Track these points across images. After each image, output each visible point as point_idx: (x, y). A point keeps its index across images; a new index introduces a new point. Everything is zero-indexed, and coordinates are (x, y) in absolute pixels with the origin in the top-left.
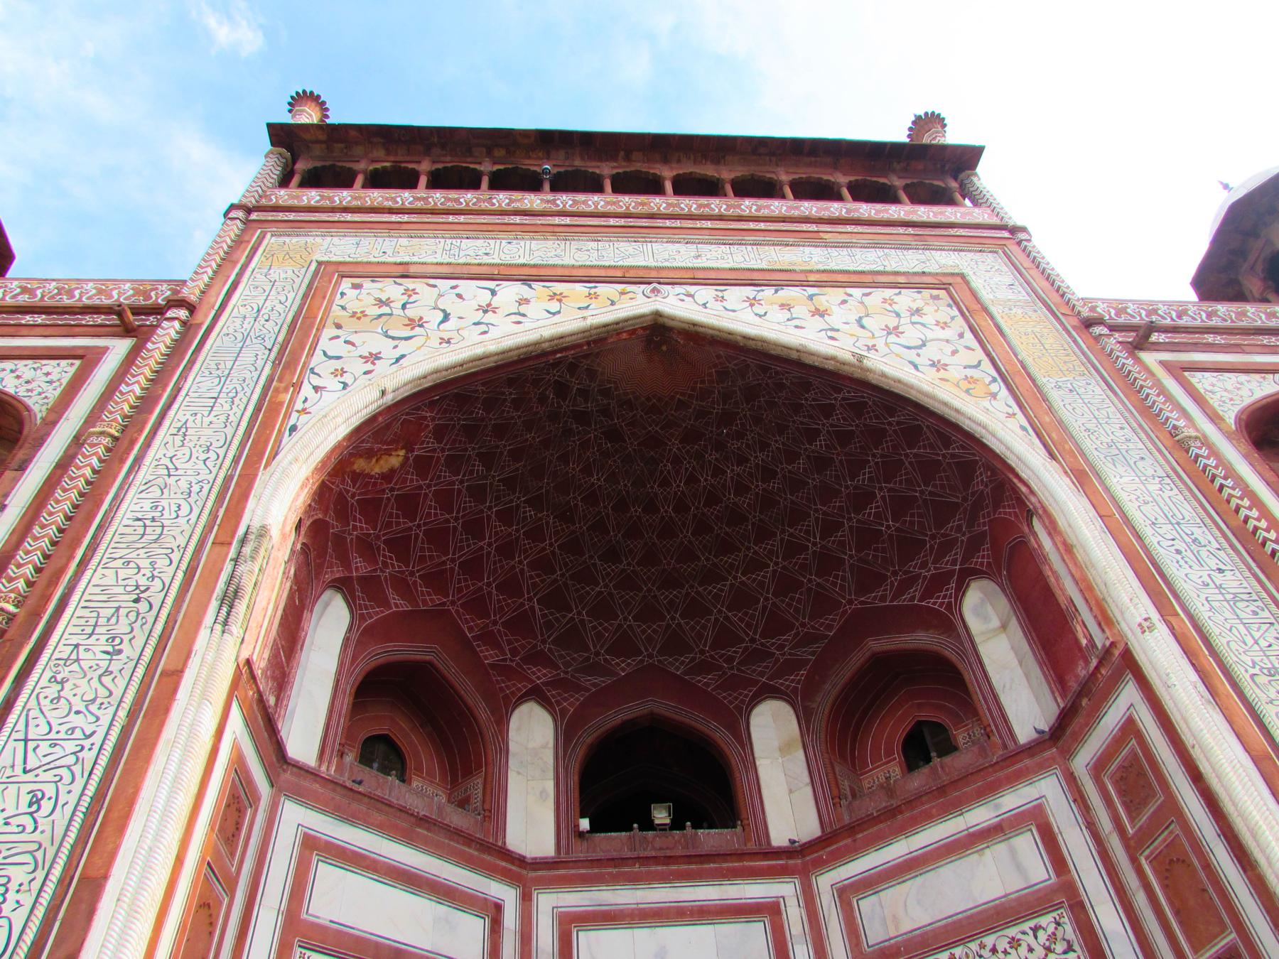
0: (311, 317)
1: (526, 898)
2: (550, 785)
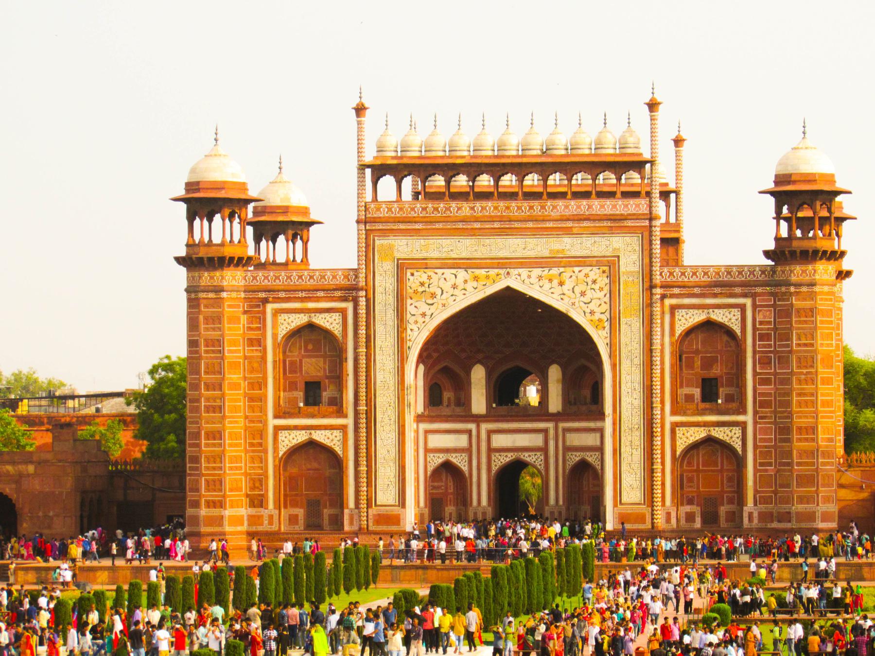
0: (402, 295)
1: (478, 427)
2: (484, 391)
